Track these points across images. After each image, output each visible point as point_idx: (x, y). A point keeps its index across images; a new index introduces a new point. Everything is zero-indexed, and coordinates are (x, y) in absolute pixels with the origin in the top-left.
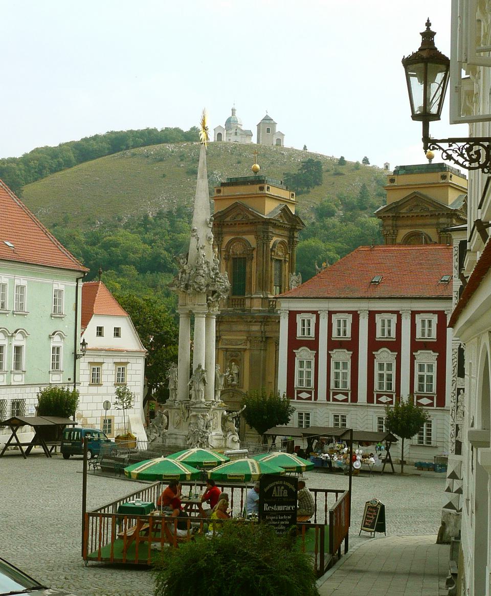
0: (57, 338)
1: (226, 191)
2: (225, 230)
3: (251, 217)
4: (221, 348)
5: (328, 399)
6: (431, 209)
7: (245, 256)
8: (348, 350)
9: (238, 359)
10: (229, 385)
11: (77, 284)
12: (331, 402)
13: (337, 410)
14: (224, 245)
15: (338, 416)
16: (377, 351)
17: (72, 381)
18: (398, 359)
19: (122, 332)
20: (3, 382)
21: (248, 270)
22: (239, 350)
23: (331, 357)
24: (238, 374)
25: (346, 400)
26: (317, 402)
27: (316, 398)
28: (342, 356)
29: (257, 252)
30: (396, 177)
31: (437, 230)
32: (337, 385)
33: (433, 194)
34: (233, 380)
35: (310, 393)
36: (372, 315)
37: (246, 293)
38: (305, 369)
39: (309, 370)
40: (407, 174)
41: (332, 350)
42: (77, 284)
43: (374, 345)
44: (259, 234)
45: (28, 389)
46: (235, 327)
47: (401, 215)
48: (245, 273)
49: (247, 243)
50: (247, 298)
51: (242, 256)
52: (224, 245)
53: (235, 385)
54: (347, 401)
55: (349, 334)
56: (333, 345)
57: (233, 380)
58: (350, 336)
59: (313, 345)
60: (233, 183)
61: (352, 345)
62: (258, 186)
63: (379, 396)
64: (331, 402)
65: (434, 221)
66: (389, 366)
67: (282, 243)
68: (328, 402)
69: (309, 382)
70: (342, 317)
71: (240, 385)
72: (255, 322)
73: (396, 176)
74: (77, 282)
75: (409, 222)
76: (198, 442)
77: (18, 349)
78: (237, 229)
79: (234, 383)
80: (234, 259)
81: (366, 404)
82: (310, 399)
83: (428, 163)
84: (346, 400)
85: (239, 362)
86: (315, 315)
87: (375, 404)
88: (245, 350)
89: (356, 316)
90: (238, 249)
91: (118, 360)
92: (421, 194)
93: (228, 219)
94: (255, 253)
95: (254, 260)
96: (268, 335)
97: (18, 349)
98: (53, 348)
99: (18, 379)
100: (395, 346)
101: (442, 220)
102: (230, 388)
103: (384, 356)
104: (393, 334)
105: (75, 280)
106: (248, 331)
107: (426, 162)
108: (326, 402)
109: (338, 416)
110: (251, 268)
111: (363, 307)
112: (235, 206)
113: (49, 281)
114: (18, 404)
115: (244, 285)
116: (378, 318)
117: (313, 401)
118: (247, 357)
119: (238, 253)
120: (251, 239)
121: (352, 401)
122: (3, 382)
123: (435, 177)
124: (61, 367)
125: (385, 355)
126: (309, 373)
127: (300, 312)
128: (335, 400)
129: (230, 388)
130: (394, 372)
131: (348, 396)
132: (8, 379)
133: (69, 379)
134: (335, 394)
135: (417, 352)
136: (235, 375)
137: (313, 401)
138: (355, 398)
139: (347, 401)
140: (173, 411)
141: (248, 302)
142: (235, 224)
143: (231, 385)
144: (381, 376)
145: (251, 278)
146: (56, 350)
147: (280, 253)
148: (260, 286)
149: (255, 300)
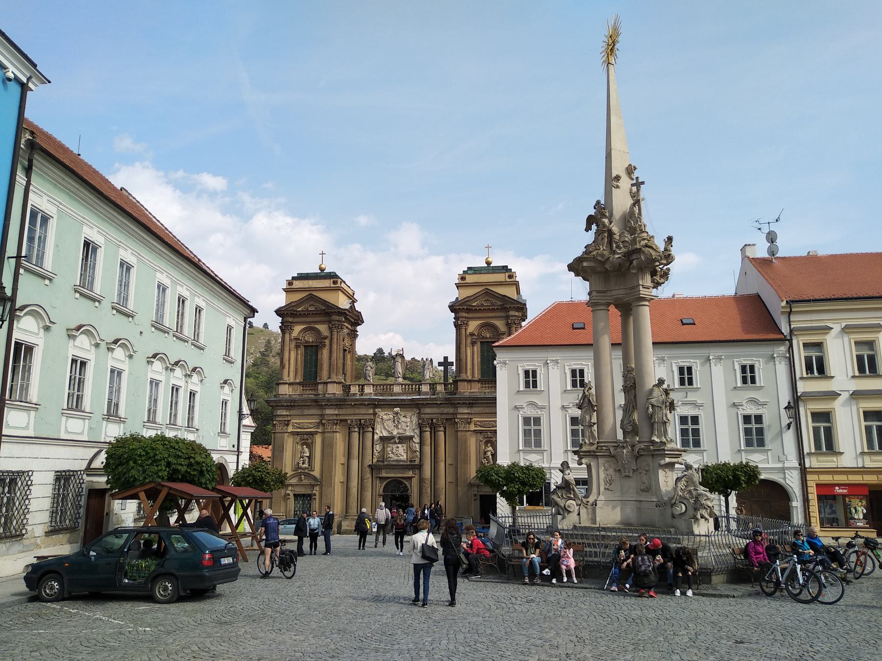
1: (297, 284)
6: (499, 303)
24: (309, 457)
46: (306, 412)
49: (318, 331)
53: (306, 468)
60: (302, 277)
65: (503, 314)
77: (192, 394)
85: (310, 446)
88: (316, 433)
90: (310, 338)
94: (327, 342)
97: (192, 394)
101: (512, 313)
118: (318, 439)
120: (323, 328)
133: (234, 446)
146: (225, 403)
149: (329, 385)
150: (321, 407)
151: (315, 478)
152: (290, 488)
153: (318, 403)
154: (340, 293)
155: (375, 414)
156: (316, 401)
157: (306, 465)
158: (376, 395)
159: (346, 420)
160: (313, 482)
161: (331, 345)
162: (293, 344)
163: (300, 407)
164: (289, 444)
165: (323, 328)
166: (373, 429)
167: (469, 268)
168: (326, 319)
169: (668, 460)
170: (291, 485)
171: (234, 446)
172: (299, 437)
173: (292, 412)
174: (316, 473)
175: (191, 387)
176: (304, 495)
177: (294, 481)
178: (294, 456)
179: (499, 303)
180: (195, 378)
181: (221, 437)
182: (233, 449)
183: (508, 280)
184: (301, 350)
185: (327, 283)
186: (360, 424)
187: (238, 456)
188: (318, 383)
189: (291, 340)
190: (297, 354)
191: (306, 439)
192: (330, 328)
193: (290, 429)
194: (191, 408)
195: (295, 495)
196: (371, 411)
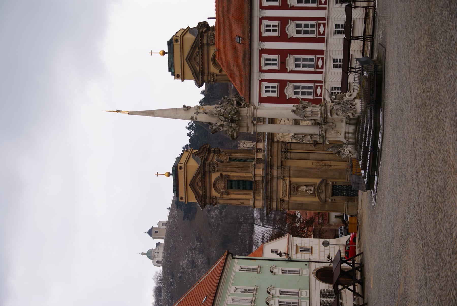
0: (275, 271)
2: (208, 195)
3: (200, 176)
4: (289, 198)
5: (321, 72)
6: (197, 50)
7: (226, 180)
8: (287, 57)
9: (296, 186)
10: (314, 193)
11: (237, 258)
12: (324, 70)
13: (330, 66)
14: (219, 195)
15: (334, 65)
16: (287, 35)
17: (307, 263)
18: (293, 19)
19: (275, 248)
20: (306, 302)
21: (235, 179)
22: (290, 185)
23: (291, 70)
24: (307, 186)
25: (322, 59)
26: (323, 81)
27: (321, 82)
28: (291, 61)
29: (224, 171)
30: (176, 73)
31: (212, 45)
32: (311, 66)
33: (187, 49)
34: (311, 190)
35: (317, 87)
36: (263, 39)
37: (251, 180)
38: (300, 90)
39: (301, 87)
40: (174, 67)
41: (287, 69)
42: (237, 258)
43: (284, 38)
44: (211, 170)
45: (313, 288)
46: (275, 188)
47: (201, 70)
48: (238, 181)
49: (217, 180)
50: (254, 178)
51: (226, 183)
52: (219, 195)
53: (314, 189)
54: (323, 58)
55: (276, 57)
56: (283, 69)
57: (311, 190)
58: (277, 56)
59: (283, 84)
61: (283, 54)
62: (179, 170)
63: (319, 34)
64: (324, 70)
65: (206, 48)
66: (299, 26)
67: (218, 157)
68: (324, 72)
69: (310, 88)
70: (263, 62)
71: (314, 185)
72: (271, 172)
73: (175, 73)
74: (235, 258)
75: (206, 65)
76: (351, 107)
78: (208, 186)
79: (312, 189)
80: (227, 189)
81: (325, 43)
82: (321, 87)
83: (167, 55)
84: (322, 59)
85: (298, 186)
86: (262, 83)
87: (325, 37)
88: (290, 181)
89: (263, 51)
90: (221, 185)
91: (295, 251)
92: (188, 56)
93: (201, 192)
94: (224, 174)
95: (229, 174)
96: (280, 164)
97: (282, 293)
98: (283, 273)
99: (305, 294)
100: (284, 21)
101: (205, 42)
102: (316, 192)
103: (291, 30)
104: (276, 23)
105: (234, 260)
106: (278, 178)
107: (167, 56)
108: (324, 74)
109: (334, 65)
110: (234, 177)
111: (257, 46)
112: (192, 185)
113: (233, 274)
114: (323, 295)
115: (246, 181)
116: (265, 34)
117: (323, 84)
118: (294, 180)
119: (223, 185)
120: (215, 176)
121: (323, 55)
122: (306, 302)
123: (177, 47)
124: (298, 269)
125: (290, 29)
126: (304, 88)
127: (260, 94)
128: (322, 68)
129: (316, 192)
130: (303, 23)
131: (319, 58)
132: (304, 299)
133: (306, 265)
134: (318, 67)
135: (288, 5)
136: (307, 189)
137: (323, 84)
138: (321, 52)
139: (323, 58)
140: (327, 136)
141: (258, 178)
142: (204, 187)
143: (314, 191)
144: (306, 32)
145: (241, 177)
146: (283, 271)
147: (225, 158)
148: (247, 170)
149: (256, 173)
150: (272, 178)
151: (321, 182)
152: (327, 199)
153: (268, 180)
154: (188, 164)
155: (278, 142)
156: (267, 183)
157: (312, 189)
158: (264, 141)
159: (282, 162)
160: (324, 184)
161: (227, 172)
162: (225, 196)
163: (271, 191)
164: (296, 199)
165: (215, 176)
166: (288, 143)
167: (170, 70)
168: (207, 175)
169: (329, 114)
170: (326, 198)
171: (306, 265)
172: (292, 193)
173: (274, 197)
174: (318, 181)
175: (278, 294)
176: (333, 190)
177: (323, 196)
178: (305, 196)
179: (197, 50)
180: (273, 292)
181: (302, 274)
182: (308, 266)
183: (179, 42)
184: (231, 191)
185: (181, 173)
186: (285, 152)
187: (311, 262)
188: (255, 180)
189: (222, 199)
190: (233, 194)
191: (294, 189)
192: (215, 172)
193: (287, 199)
194: (289, 293)
195: (333, 195)
196: (276, 145)
